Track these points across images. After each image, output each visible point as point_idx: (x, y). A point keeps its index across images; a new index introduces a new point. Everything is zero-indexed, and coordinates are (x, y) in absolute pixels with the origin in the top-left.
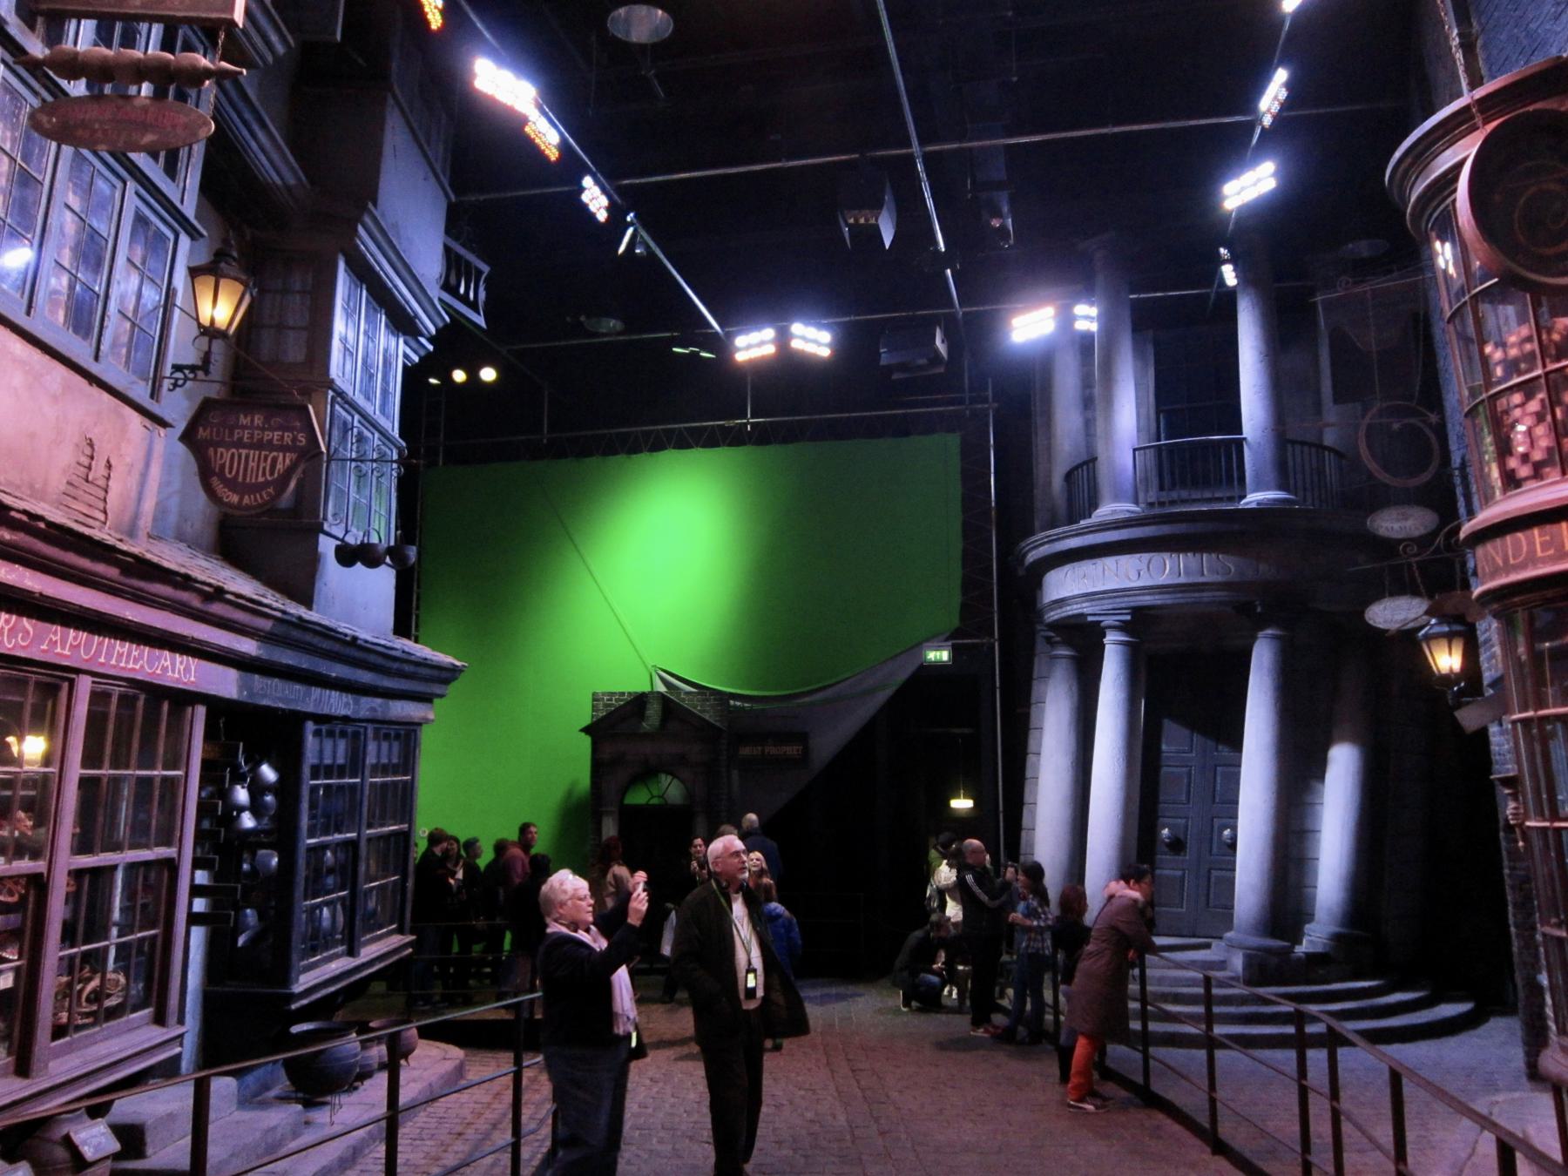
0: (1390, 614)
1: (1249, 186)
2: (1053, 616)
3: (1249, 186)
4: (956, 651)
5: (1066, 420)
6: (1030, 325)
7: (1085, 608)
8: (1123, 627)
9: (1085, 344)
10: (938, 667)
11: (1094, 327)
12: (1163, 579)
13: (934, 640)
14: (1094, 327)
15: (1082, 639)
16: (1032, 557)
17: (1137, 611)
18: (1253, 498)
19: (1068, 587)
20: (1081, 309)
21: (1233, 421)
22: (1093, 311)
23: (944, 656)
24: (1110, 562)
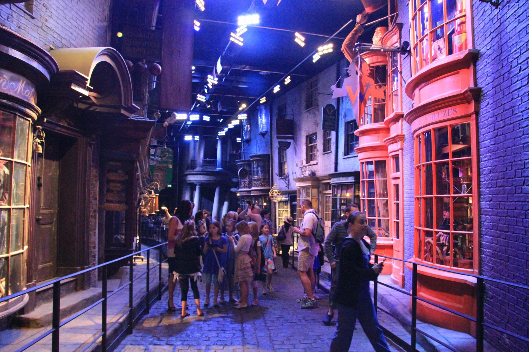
0: (233, 190)
1: (222, 133)
2: (189, 182)
3: (222, 133)
4: (172, 185)
5: (191, 151)
6: (188, 138)
7: (194, 182)
8: (199, 185)
9: (195, 141)
10: (169, 187)
11: (198, 139)
12: (206, 179)
13: (170, 184)
14: (198, 139)
15: (193, 186)
16: (186, 173)
17: (202, 183)
18: (218, 169)
19: (192, 178)
20: (196, 137)
21: (216, 158)
22: (198, 137)
23: (170, 186)
24: (198, 176)
